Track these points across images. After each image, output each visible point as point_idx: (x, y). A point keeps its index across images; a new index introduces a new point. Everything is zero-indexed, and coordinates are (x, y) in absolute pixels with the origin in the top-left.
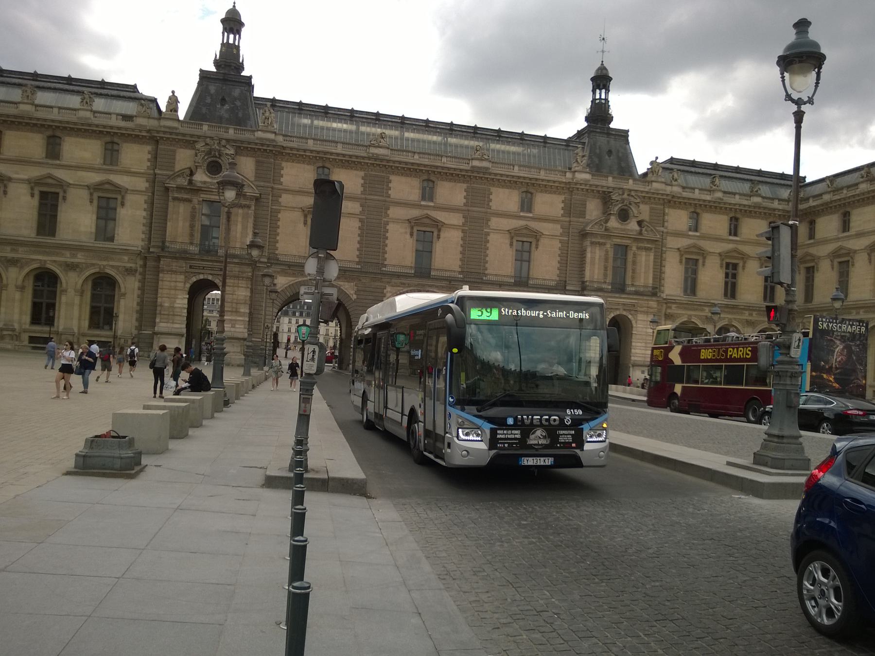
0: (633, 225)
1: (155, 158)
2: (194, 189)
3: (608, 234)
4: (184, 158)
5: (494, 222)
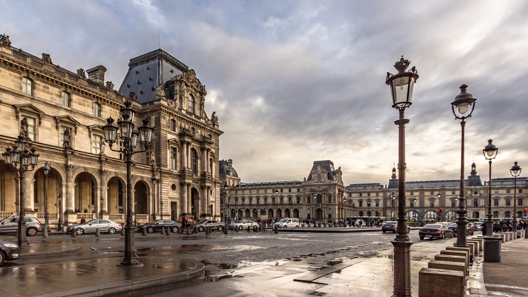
0: (478, 195)
1: (384, 195)
2: (390, 198)
3: (472, 197)
4: (388, 194)
5: (447, 197)
